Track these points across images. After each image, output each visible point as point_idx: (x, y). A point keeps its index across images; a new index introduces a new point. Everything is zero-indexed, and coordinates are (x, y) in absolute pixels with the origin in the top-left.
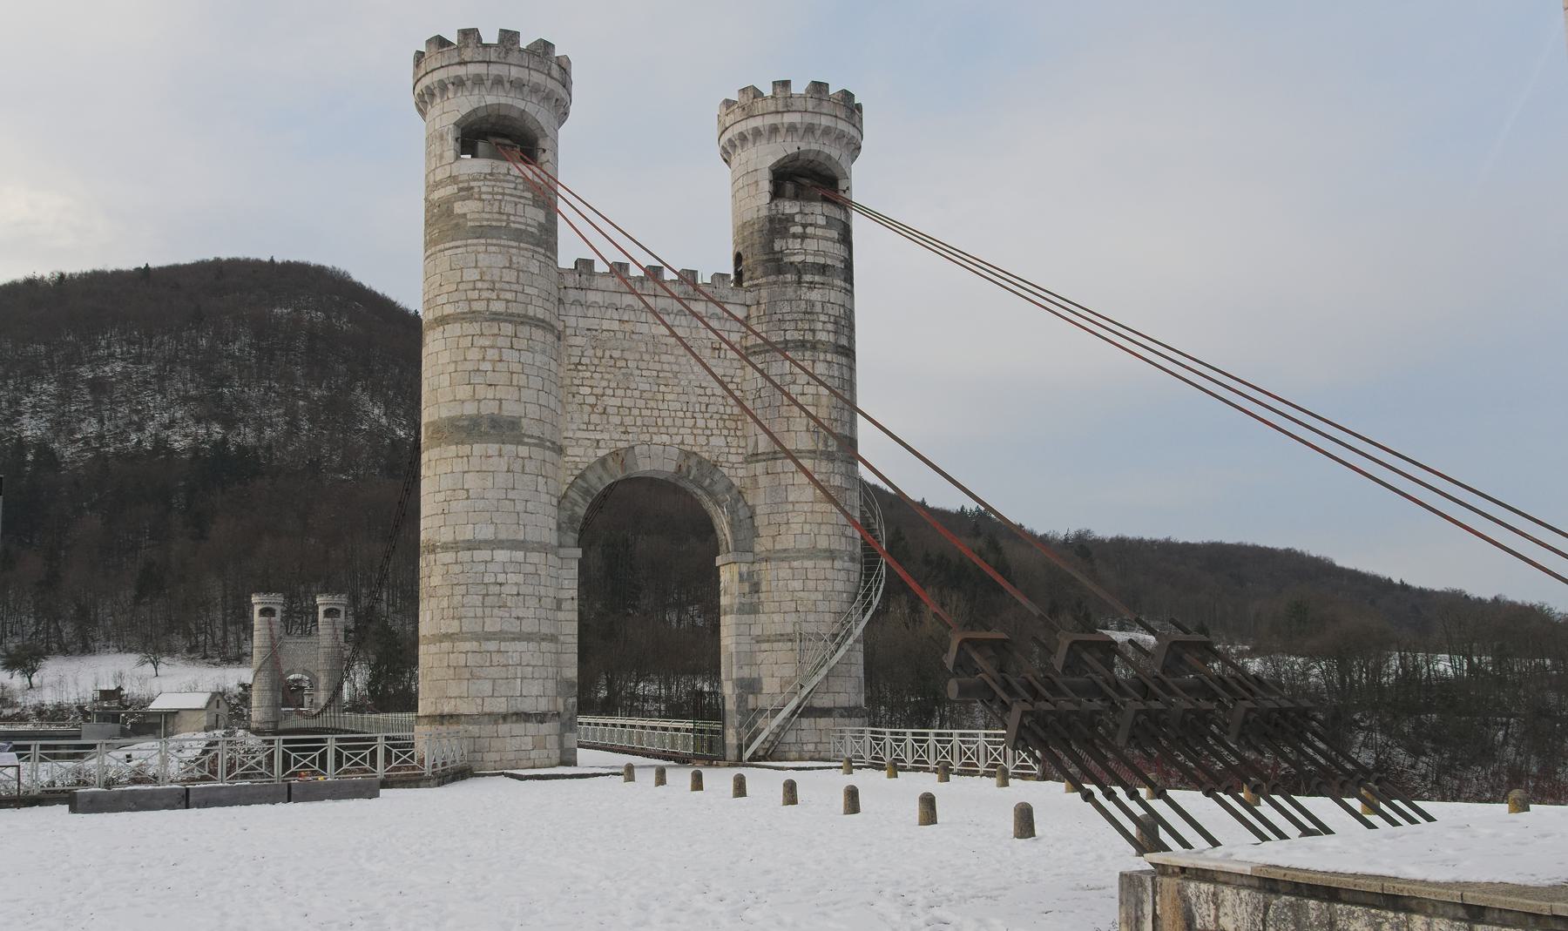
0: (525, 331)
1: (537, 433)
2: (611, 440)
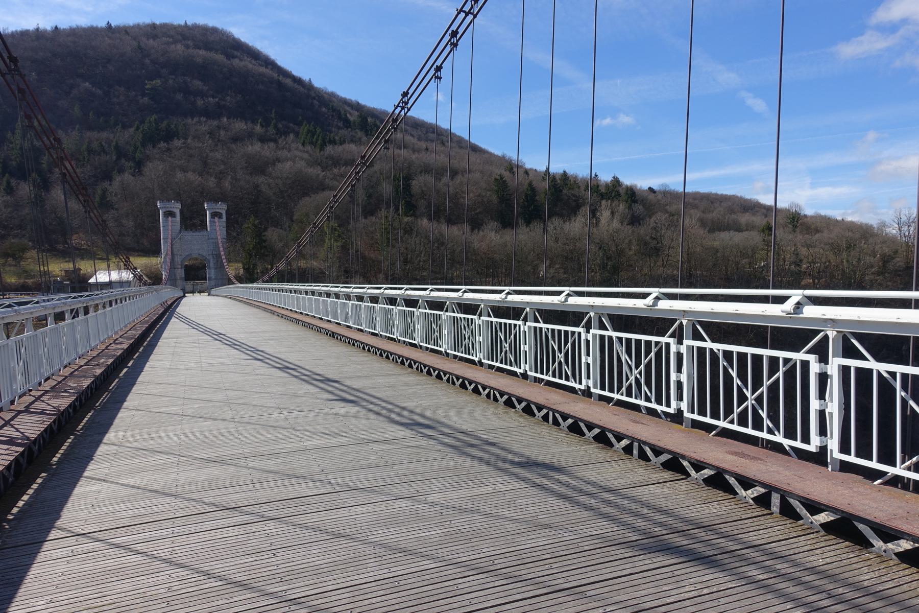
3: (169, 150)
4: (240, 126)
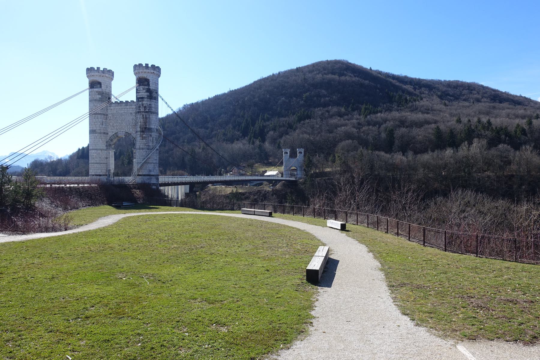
0: (97, 116)
1: (99, 131)
2: (115, 131)
3: (304, 124)
4: (335, 109)
